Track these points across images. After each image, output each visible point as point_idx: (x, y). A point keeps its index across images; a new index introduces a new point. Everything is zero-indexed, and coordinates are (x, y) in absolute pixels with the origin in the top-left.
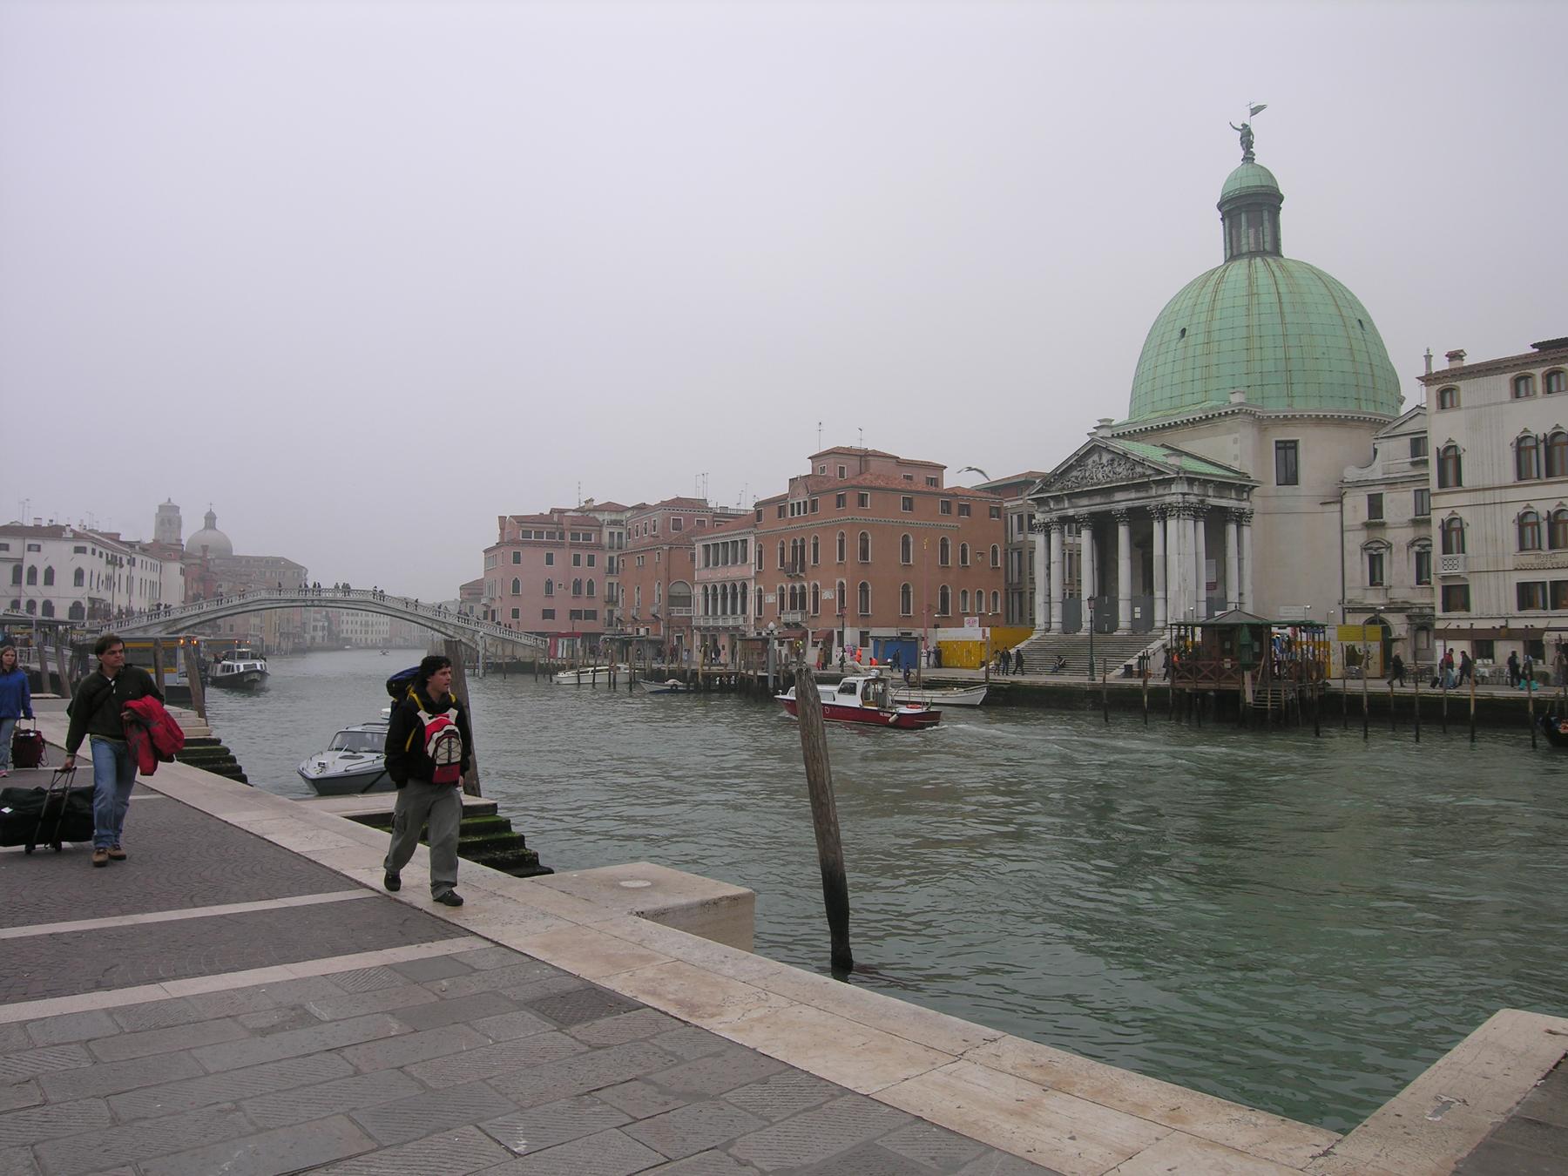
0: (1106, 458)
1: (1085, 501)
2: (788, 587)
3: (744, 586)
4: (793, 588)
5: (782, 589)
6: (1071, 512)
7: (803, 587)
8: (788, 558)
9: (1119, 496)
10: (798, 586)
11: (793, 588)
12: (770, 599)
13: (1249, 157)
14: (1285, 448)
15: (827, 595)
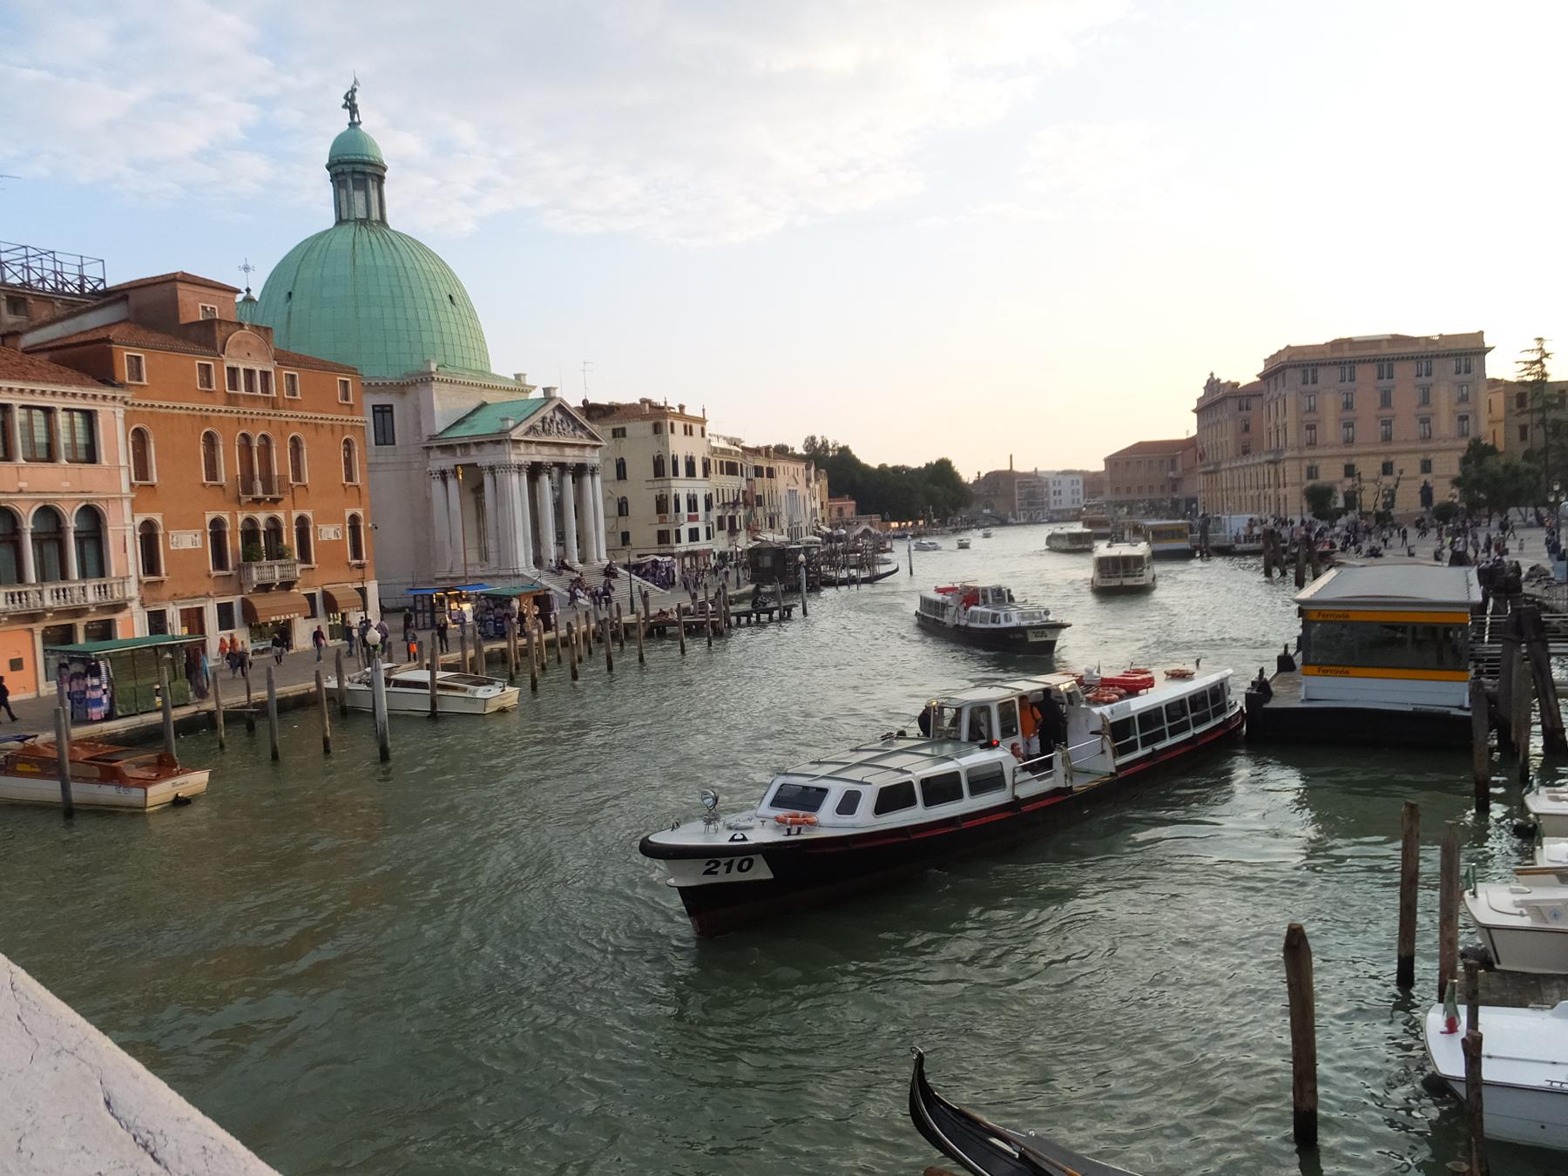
0: (558, 416)
1: (545, 450)
2: (235, 521)
3: (93, 517)
4: (251, 521)
5: (217, 524)
6: (537, 459)
7: (274, 520)
8: (229, 466)
9: (568, 451)
10: (261, 517)
11: (251, 521)
12: (186, 541)
13: (353, 125)
14: (383, 412)
15: (328, 533)
